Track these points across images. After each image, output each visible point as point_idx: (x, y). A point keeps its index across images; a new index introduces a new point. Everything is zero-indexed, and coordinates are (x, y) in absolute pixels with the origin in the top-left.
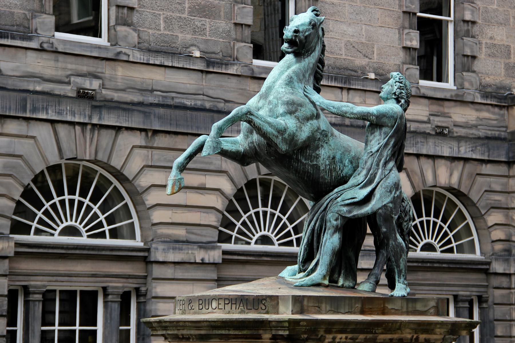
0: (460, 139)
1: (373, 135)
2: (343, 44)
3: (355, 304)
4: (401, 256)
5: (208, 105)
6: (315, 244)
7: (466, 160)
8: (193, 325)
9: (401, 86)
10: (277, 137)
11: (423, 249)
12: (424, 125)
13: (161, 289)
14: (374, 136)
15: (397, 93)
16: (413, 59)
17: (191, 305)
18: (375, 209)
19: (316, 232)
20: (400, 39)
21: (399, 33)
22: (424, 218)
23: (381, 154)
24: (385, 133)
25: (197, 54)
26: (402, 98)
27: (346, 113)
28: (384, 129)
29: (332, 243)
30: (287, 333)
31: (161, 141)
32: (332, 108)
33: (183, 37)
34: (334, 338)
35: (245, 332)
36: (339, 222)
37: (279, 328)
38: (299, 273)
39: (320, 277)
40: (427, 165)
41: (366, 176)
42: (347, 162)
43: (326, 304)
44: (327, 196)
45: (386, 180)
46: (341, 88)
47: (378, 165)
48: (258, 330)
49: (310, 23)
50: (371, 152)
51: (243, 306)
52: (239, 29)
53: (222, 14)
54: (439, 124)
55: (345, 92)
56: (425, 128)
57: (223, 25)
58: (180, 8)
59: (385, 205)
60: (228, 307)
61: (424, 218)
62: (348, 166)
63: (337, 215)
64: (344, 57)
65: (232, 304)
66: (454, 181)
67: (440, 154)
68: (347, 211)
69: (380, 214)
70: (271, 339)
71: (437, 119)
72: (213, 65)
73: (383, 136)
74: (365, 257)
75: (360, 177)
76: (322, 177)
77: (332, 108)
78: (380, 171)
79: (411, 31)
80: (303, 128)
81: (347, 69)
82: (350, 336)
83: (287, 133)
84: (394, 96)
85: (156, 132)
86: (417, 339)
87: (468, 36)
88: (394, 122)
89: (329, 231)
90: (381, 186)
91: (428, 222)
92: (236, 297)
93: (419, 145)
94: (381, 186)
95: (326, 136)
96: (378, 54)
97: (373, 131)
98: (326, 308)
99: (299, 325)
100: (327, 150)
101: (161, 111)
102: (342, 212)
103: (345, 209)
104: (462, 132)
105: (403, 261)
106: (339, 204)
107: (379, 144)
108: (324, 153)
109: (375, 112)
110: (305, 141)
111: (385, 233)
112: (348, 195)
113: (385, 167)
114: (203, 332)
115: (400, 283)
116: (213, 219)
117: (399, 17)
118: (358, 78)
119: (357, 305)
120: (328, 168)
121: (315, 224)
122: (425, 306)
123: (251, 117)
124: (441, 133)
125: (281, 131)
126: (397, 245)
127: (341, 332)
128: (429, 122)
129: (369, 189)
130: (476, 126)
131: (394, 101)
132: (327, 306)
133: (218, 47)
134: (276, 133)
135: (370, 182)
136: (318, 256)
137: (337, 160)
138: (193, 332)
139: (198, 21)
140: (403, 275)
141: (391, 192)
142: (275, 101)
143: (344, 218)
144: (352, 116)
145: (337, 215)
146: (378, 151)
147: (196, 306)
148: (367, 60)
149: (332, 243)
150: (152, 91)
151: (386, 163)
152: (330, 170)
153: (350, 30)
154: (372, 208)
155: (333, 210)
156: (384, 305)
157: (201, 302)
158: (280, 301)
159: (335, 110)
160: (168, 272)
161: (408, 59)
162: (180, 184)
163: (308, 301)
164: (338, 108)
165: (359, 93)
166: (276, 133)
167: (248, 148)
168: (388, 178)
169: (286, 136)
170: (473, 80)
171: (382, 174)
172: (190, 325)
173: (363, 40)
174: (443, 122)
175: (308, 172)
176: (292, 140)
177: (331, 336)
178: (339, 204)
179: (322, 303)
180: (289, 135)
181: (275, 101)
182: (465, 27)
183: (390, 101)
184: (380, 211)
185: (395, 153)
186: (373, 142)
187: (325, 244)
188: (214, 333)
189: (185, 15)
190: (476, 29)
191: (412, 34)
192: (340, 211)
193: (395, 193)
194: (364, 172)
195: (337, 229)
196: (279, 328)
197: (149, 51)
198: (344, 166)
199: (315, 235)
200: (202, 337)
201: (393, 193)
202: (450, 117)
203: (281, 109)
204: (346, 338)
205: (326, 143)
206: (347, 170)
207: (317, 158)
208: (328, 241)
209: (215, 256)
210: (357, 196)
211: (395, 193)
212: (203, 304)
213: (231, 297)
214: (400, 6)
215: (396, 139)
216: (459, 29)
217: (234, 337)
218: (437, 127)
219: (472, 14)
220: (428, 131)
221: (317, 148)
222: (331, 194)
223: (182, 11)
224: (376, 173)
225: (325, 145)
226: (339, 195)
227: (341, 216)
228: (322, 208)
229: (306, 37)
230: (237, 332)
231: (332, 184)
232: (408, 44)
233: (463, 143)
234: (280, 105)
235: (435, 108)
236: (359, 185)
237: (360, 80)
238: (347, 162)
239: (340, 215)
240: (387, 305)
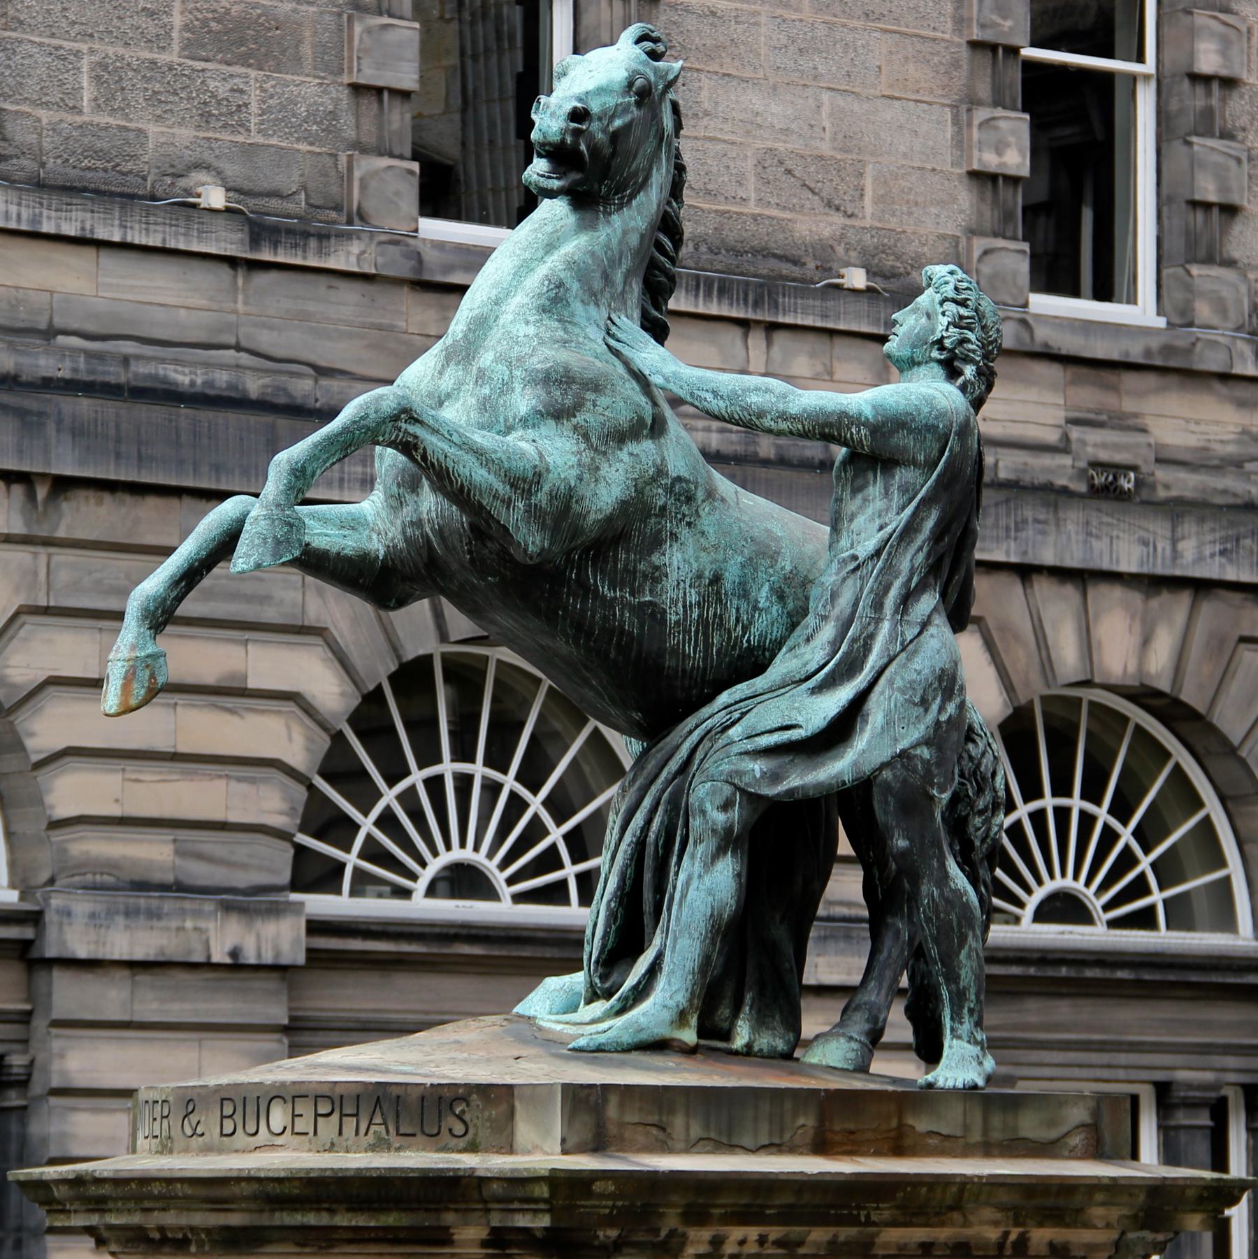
0: (1177, 509)
1: (860, 496)
2: (751, 162)
3: (795, 1116)
4: (963, 940)
5: (254, 386)
6: (648, 895)
7: (1201, 587)
8: (202, 1192)
9: (961, 317)
10: (508, 503)
11: (1041, 915)
12: (1047, 461)
13: (82, 1061)
14: (865, 500)
15: (947, 343)
16: (1007, 217)
17: (194, 1118)
18: (867, 769)
19: (650, 850)
20: (960, 143)
21: (956, 121)
22: (1048, 802)
23: (889, 568)
24: (904, 489)
25: (215, 198)
26: (967, 360)
27: (761, 414)
28: (902, 475)
29: (710, 892)
30: (544, 1221)
31: (85, 517)
32: (709, 396)
33: (164, 135)
34: (717, 1242)
35: (390, 1219)
36: (735, 814)
37: (516, 1205)
38: (588, 1002)
39: (666, 1015)
40: (1058, 607)
41: (835, 645)
42: (763, 595)
43: (687, 1115)
44: (691, 721)
45: (908, 659)
46: (744, 324)
47: (878, 605)
48: (437, 1210)
49: (630, 84)
50: (855, 558)
51: (385, 1123)
52: (369, 105)
53: (307, 50)
54: (1104, 456)
55: (757, 339)
56: (1049, 470)
57: (310, 91)
58: (151, 27)
59: (903, 752)
60: (328, 1128)
61: (1048, 802)
62: (767, 610)
63: (728, 790)
64: (752, 208)
65: (342, 1115)
66: (1158, 665)
67: (1106, 565)
68: (763, 774)
69: (887, 787)
70: (484, 1244)
71: (1093, 436)
72: (270, 238)
73: (896, 499)
74: (831, 945)
75: (811, 651)
76: (675, 650)
77: (709, 396)
78: (886, 626)
79: (999, 112)
80: (605, 469)
81: (764, 252)
82: (775, 1233)
83: (546, 488)
84: (935, 354)
85: (63, 485)
86: (1022, 1242)
87: (1209, 133)
88: (936, 446)
89: (700, 849)
90: (891, 682)
91: (1062, 814)
92: (359, 1090)
93: (1029, 532)
94: (891, 682)
95: (690, 499)
96: (878, 200)
97: (859, 482)
98: (687, 1129)
99: (589, 1194)
100: (690, 551)
101: (84, 406)
102: (746, 779)
103: (757, 767)
104: (1185, 483)
105: (969, 957)
106: (736, 749)
107: (881, 528)
108: (680, 561)
109: (868, 412)
110: (609, 519)
111: (904, 854)
112: (769, 714)
113: (905, 612)
114: (235, 1219)
115: (959, 1037)
116: (272, 804)
117: (956, 64)
118: (803, 288)
119: (801, 1121)
120: (695, 615)
121: (649, 821)
122: (1052, 1123)
123: (412, 429)
124: (1108, 489)
125: (524, 480)
126: (947, 901)
127: (743, 1217)
128: (1063, 447)
129: (844, 694)
130: (1236, 464)
131: (938, 371)
132: (692, 1122)
133: (292, 171)
134: (503, 489)
135: (849, 668)
136: (657, 941)
137: (729, 586)
138: (200, 1219)
139: (219, 78)
140: (971, 1011)
141: (925, 703)
142: (501, 370)
143: (752, 799)
144: (783, 426)
145: (728, 790)
146: (877, 553)
147: (210, 1123)
148: (838, 219)
149: (710, 892)
150: (51, 333)
151: (907, 599)
152: (703, 623)
153: (777, 111)
154: (855, 764)
155: (712, 770)
156: (900, 1119)
157: (228, 1110)
158: (517, 1104)
159: (721, 403)
160: (110, 998)
161: (989, 216)
162: (152, 676)
163: (622, 1106)
164: (733, 397)
165: (810, 340)
166: (503, 489)
167: (401, 544)
168: (915, 652)
169: (541, 498)
170: (1226, 293)
171: (893, 637)
172: (189, 1191)
173: (825, 148)
174: (1117, 447)
175: (622, 631)
176: (561, 513)
177: (706, 1234)
178: (736, 749)
179: (672, 1112)
180: (553, 496)
181: (501, 370)
182: (1197, 100)
183: (923, 370)
184: (887, 774)
185: (940, 560)
186: (860, 520)
187: (684, 896)
188: (278, 1223)
189: (172, 56)
190: (1237, 108)
191: (1003, 124)
192: (740, 773)
193: (941, 709)
194: (828, 632)
195: (727, 842)
196: (516, 1205)
197: (40, 185)
198: (755, 608)
199: (649, 862)
200: (232, 1238)
201: (935, 707)
202: (1144, 431)
203: (523, 402)
204: (762, 1241)
205: (689, 524)
206: (764, 625)
207: (656, 581)
208: (695, 883)
209: (281, 939)
210: (800, 720)
211: (941, 709)
212: (238, 1117)
213: (339, 1090)
214: (960, 22)
215: (943, 511)
216: (1174, 106)
217: (350, 1235)
218: (1095, 464)
219: (1224, 53)
220: (1061, 481)
221: (656, 542)
222: (706, 711)
223: (160, 41)
224: (872, 636)
225: (684, 532)
226: (736, 715)
227: (743, 792)
228: (674, 765)
229: (615, 137)
230: (361, 1220)
231: (710, 676)
232: (990, 161)
233: (1189, 527)
234: (518, 387)
235: (1089, 396)
236: (808, 678)
237: (815, 294)
238: (763, 595)
239: (737, 788)
240: (910, 1121)
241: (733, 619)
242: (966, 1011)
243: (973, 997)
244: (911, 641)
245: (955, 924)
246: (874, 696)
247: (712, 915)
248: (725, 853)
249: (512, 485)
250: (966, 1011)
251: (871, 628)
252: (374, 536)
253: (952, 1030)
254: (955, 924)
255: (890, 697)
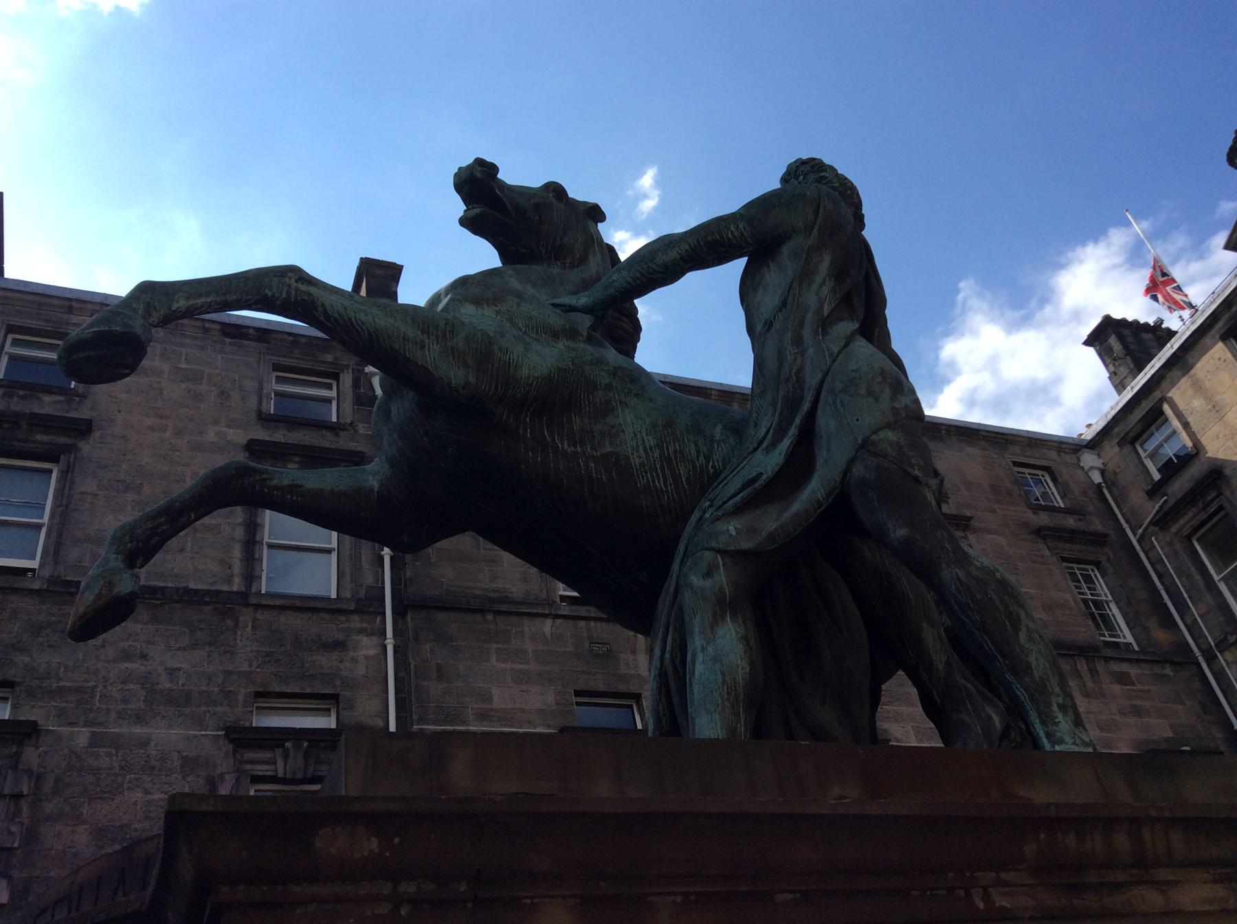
28: (786, 250)
36: (722, 577)
47: (798, 341)
68: (739, 531)
103: (732, 527)
105: (1031, 639)
113: (825, 333)
120: (657, 454)
123: (304, 288)
140: (1062, 707)
184: (858, 470)
195: (723, 607)
205: (637, 395)
208: (700, 657)
210: (759, 470)
224: (800, 370)
239: (718, 551)
241: (693, 451)
242: (1055, 708)
243: (1057, 690)
244: (839, 353)
245: (998, 602)
246: (819, 412)
247: (724, 682)
248: (723, 619)
249: (423, 332)
250: (1055, 708)
251: (799, 361)
252: (370, 478)
253: (1048, 735)
254: (998, 602)
255: (834, 403)
